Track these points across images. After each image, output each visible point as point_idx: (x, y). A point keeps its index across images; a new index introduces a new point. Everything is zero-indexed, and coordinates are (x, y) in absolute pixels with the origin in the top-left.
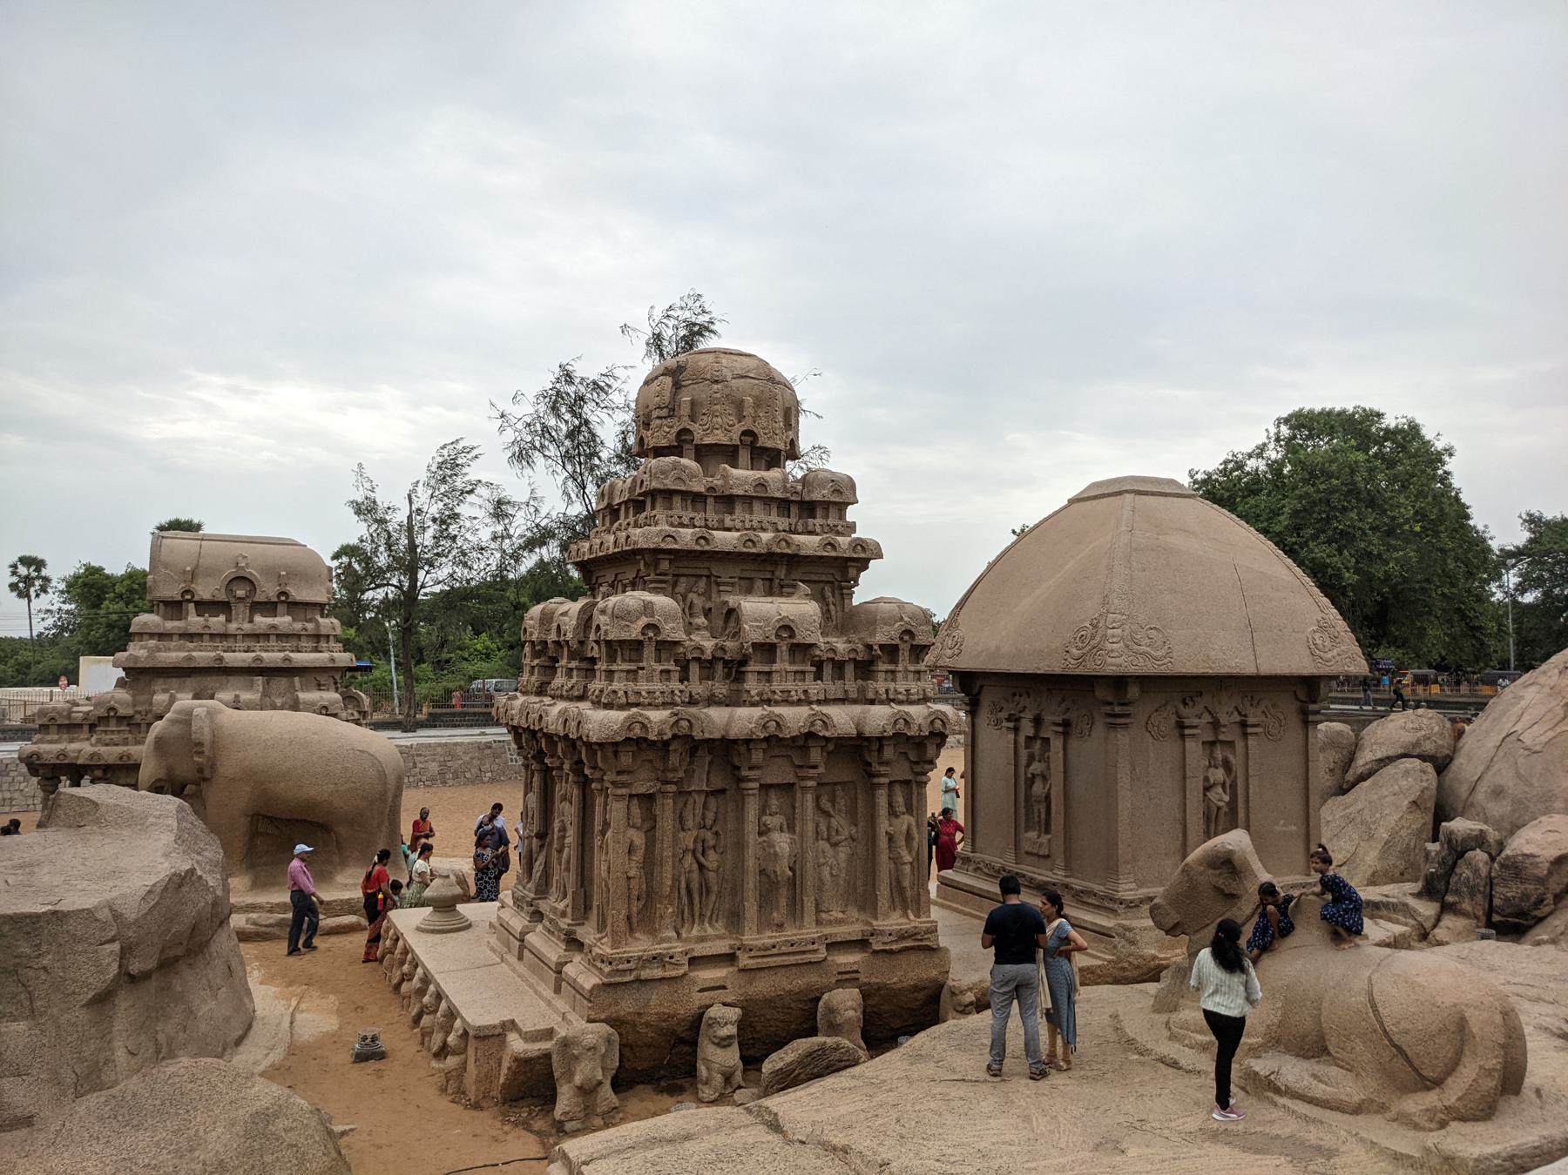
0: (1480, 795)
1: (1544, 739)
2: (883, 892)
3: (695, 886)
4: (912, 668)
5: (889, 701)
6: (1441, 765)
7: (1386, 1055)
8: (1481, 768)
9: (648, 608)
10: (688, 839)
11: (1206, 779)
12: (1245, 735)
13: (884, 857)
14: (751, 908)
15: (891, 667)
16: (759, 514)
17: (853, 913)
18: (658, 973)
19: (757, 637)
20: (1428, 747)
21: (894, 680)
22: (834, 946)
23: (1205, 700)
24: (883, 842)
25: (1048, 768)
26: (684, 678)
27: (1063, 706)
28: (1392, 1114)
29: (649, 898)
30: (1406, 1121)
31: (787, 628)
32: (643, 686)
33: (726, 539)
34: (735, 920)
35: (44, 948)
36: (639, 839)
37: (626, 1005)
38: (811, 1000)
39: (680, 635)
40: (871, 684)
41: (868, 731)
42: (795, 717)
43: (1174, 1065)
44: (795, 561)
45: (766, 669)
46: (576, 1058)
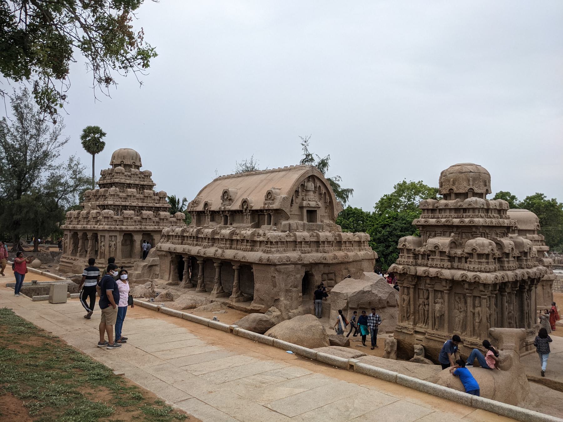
2: (469, 329)
4: (477, 261)
10: (421, 301)
13: (470, 318)
14: (430, 323)
16: (448, 214)
18: (406, 331)
19: (430, 249)
24: (469, 314)
31: (436, 246)
32: (403, 260)
33: (433, 221)
36: (406, 297)
37: (401, 337)
39: (412, 248)
41: (455, 278)
42: (433, 271)
44: (458, 227)
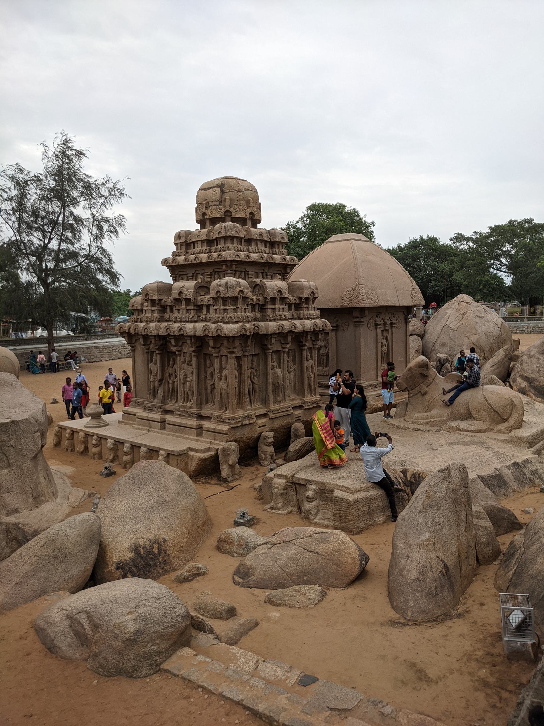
0: (437, 347)
1: (457, 326)
3: (251, 390)
5: (274, 320)
6: (422, 336)
7: (493, 414)
8: (436, 338)
9: (239, 284)
11: (382, 343)
12: (392, 327)
15: (307, 306)
17: (295, 396)
18: (247, 422)
20: (418, 331)
21: (308, 310)
22: (295, 408)
23: (382, 316)
25: (328, 342)
26: (290, 310)
27: (335, 320)
28: (495, 431)
29: (240, 395)
30: (501, 432)
34: (265, 402)
35: (11, 437)
38: (287, 428)
40: (302, 312)
43: (419, 430)
45: (274, 307)
46: (229, 454)
